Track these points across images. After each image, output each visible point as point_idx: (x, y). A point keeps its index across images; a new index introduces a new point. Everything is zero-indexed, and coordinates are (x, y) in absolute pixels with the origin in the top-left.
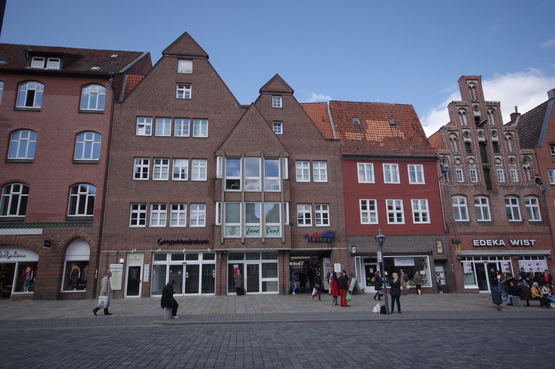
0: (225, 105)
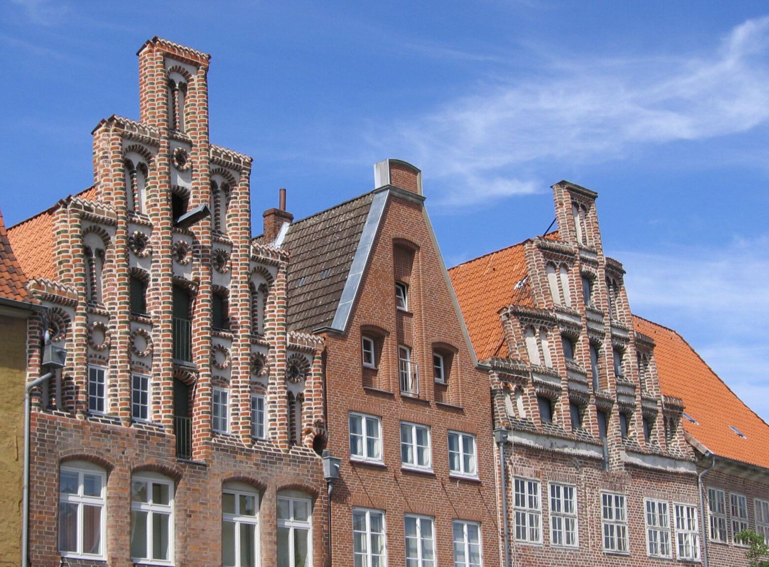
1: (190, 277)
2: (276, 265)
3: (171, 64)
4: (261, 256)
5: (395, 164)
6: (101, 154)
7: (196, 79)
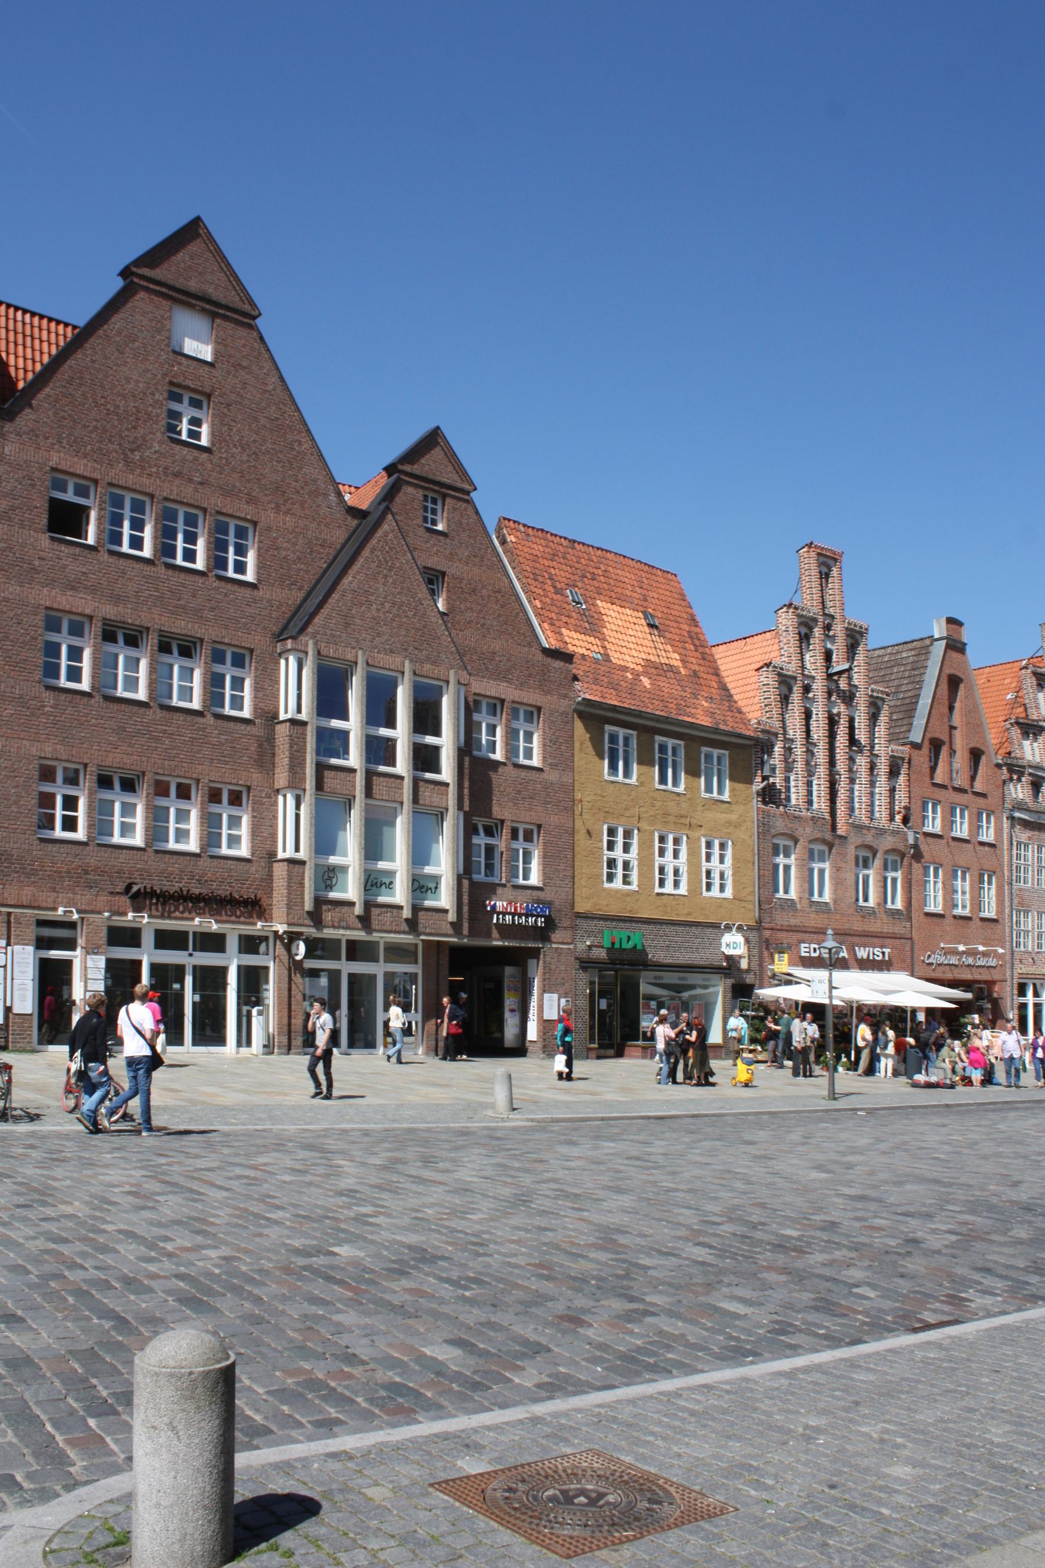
0: (302, 488)
1: (835, 711)
2: (883, 700)
3: (822, 559)
4: (875, 694)
5: (951, 621)
6: (784, 628)
7: (835, 572)
